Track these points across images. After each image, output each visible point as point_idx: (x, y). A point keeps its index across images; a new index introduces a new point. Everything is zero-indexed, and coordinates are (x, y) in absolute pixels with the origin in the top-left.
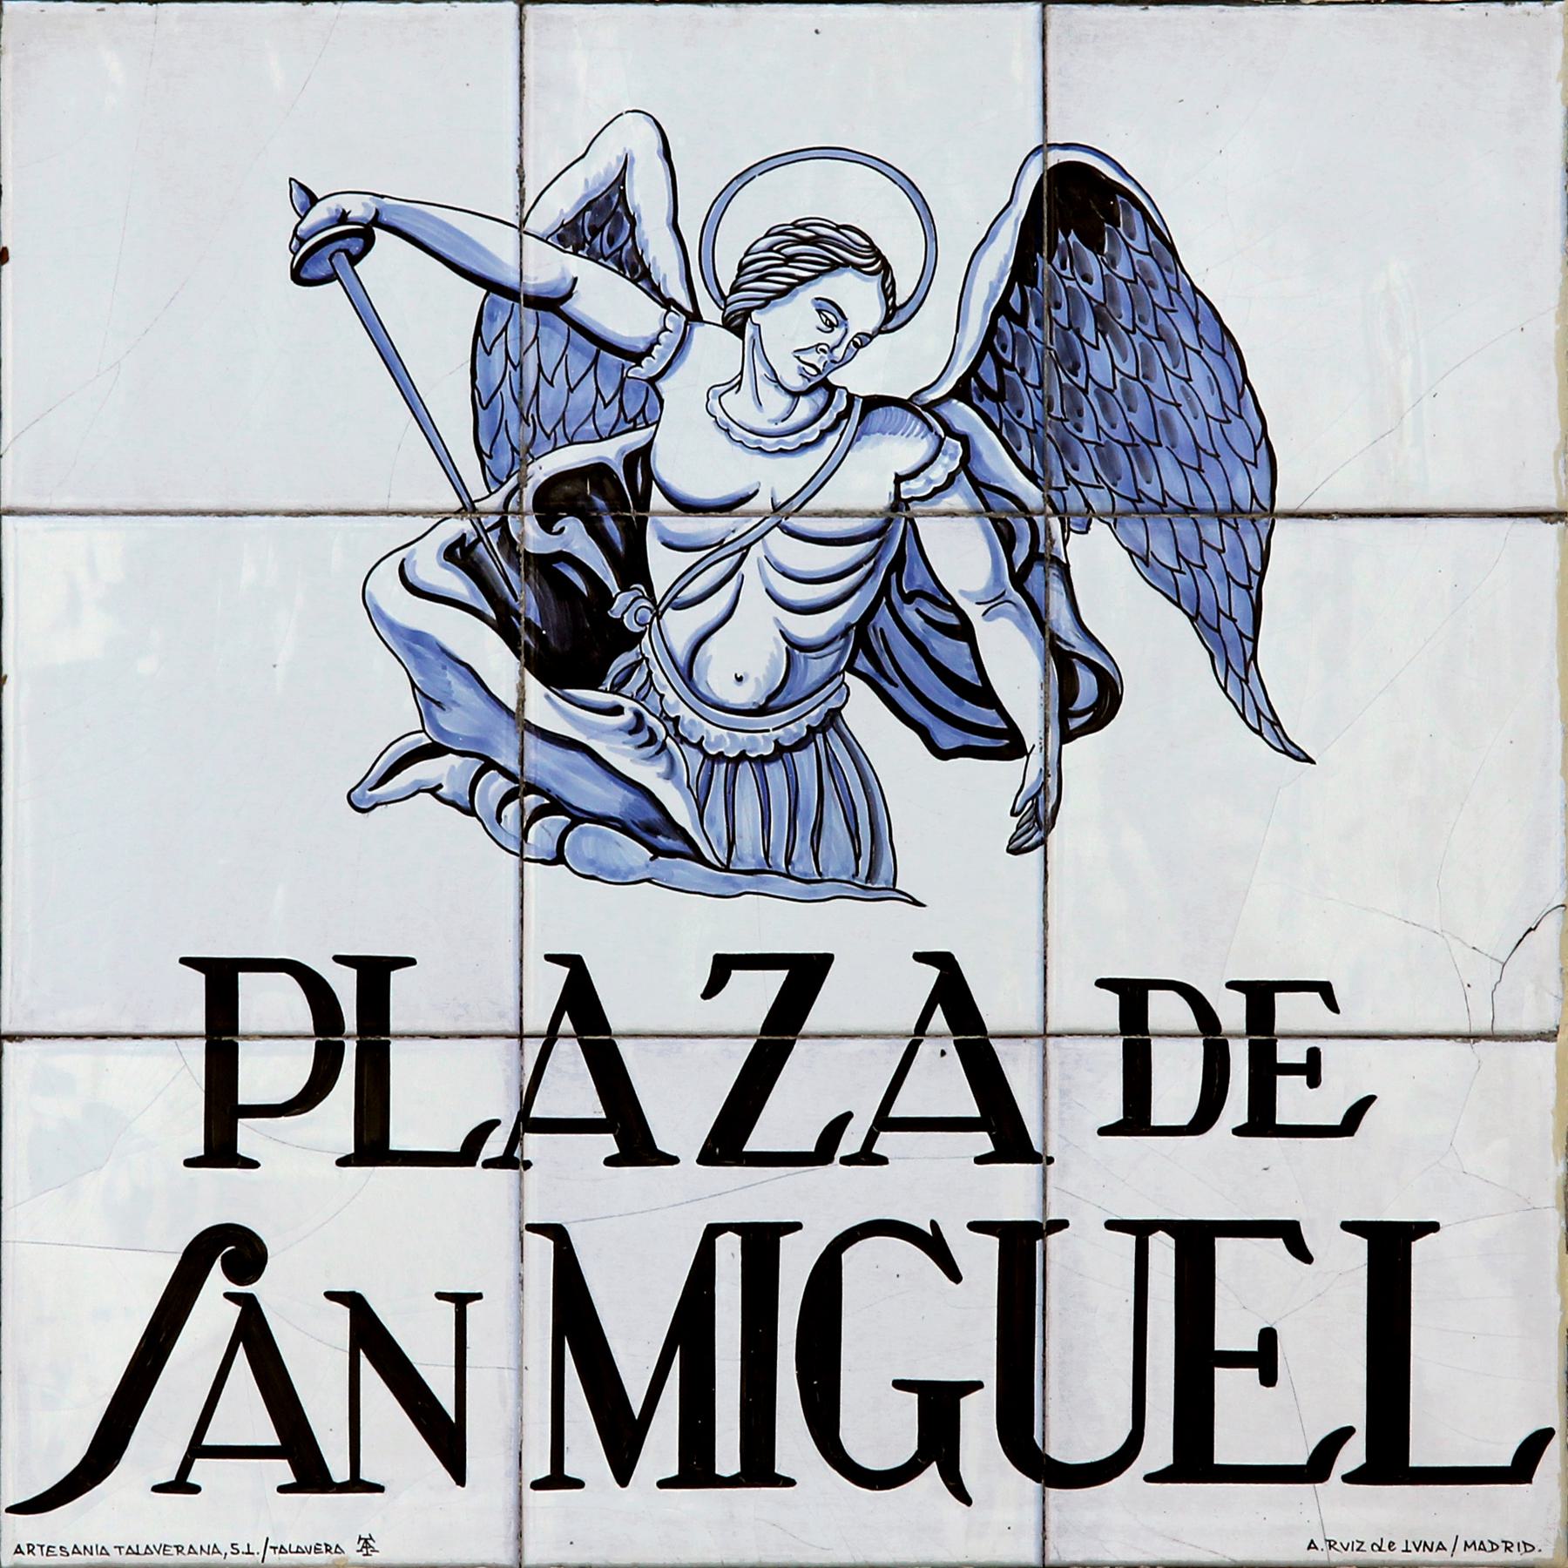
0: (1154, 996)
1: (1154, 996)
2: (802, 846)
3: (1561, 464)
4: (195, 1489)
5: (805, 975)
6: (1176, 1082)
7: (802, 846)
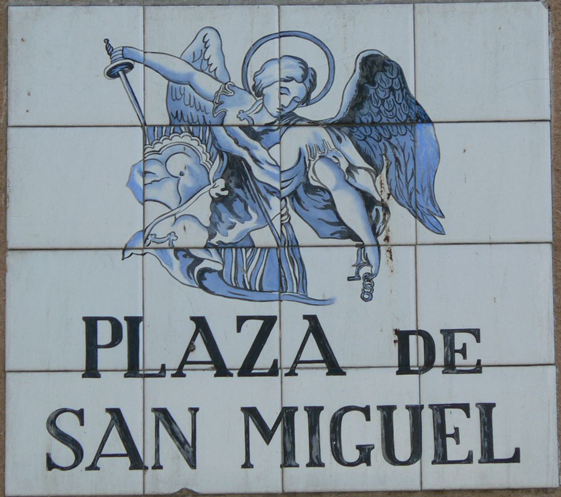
0: (99, 322)
1: (99, 322)
2: (301, 289)
3: (382, 55)
4: (98, 469)
5: (269, 322)
6: (416, 356)
7: (301, 289)
